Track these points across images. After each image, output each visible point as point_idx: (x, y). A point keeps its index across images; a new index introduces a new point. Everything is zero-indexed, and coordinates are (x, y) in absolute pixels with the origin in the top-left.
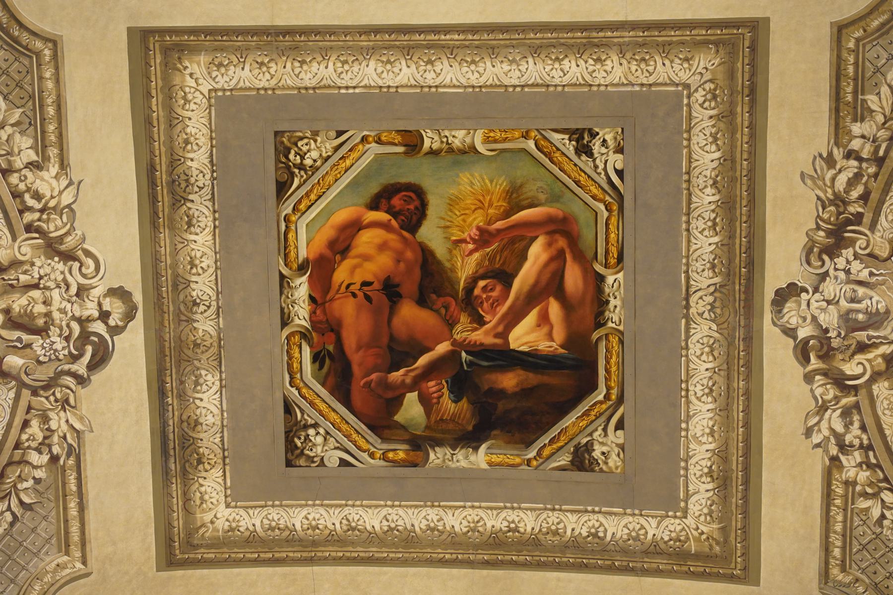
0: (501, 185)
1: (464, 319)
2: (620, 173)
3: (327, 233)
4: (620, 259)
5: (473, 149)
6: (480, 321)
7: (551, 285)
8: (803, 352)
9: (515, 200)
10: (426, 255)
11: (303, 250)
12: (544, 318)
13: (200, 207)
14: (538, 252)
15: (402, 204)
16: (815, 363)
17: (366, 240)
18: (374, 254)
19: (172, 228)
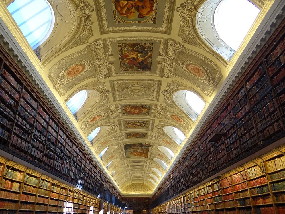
0: (129, 18)
1: (133, 4)
2: (115, 20)
3: (150, 14)
4: (114, 11)
5: (132, 21)
6: (131, 4)
7: (122, 8)
8: (89, 5)
9: (127, 17)
10: (138, 11)
11: (154, 13)
12: (123, 4)
13: (166, 18)
14: (124, 11)
15: (141, 16)
16: (87, 4)
17: (146, 13)
18: (144, 12)
19: (169, 16)
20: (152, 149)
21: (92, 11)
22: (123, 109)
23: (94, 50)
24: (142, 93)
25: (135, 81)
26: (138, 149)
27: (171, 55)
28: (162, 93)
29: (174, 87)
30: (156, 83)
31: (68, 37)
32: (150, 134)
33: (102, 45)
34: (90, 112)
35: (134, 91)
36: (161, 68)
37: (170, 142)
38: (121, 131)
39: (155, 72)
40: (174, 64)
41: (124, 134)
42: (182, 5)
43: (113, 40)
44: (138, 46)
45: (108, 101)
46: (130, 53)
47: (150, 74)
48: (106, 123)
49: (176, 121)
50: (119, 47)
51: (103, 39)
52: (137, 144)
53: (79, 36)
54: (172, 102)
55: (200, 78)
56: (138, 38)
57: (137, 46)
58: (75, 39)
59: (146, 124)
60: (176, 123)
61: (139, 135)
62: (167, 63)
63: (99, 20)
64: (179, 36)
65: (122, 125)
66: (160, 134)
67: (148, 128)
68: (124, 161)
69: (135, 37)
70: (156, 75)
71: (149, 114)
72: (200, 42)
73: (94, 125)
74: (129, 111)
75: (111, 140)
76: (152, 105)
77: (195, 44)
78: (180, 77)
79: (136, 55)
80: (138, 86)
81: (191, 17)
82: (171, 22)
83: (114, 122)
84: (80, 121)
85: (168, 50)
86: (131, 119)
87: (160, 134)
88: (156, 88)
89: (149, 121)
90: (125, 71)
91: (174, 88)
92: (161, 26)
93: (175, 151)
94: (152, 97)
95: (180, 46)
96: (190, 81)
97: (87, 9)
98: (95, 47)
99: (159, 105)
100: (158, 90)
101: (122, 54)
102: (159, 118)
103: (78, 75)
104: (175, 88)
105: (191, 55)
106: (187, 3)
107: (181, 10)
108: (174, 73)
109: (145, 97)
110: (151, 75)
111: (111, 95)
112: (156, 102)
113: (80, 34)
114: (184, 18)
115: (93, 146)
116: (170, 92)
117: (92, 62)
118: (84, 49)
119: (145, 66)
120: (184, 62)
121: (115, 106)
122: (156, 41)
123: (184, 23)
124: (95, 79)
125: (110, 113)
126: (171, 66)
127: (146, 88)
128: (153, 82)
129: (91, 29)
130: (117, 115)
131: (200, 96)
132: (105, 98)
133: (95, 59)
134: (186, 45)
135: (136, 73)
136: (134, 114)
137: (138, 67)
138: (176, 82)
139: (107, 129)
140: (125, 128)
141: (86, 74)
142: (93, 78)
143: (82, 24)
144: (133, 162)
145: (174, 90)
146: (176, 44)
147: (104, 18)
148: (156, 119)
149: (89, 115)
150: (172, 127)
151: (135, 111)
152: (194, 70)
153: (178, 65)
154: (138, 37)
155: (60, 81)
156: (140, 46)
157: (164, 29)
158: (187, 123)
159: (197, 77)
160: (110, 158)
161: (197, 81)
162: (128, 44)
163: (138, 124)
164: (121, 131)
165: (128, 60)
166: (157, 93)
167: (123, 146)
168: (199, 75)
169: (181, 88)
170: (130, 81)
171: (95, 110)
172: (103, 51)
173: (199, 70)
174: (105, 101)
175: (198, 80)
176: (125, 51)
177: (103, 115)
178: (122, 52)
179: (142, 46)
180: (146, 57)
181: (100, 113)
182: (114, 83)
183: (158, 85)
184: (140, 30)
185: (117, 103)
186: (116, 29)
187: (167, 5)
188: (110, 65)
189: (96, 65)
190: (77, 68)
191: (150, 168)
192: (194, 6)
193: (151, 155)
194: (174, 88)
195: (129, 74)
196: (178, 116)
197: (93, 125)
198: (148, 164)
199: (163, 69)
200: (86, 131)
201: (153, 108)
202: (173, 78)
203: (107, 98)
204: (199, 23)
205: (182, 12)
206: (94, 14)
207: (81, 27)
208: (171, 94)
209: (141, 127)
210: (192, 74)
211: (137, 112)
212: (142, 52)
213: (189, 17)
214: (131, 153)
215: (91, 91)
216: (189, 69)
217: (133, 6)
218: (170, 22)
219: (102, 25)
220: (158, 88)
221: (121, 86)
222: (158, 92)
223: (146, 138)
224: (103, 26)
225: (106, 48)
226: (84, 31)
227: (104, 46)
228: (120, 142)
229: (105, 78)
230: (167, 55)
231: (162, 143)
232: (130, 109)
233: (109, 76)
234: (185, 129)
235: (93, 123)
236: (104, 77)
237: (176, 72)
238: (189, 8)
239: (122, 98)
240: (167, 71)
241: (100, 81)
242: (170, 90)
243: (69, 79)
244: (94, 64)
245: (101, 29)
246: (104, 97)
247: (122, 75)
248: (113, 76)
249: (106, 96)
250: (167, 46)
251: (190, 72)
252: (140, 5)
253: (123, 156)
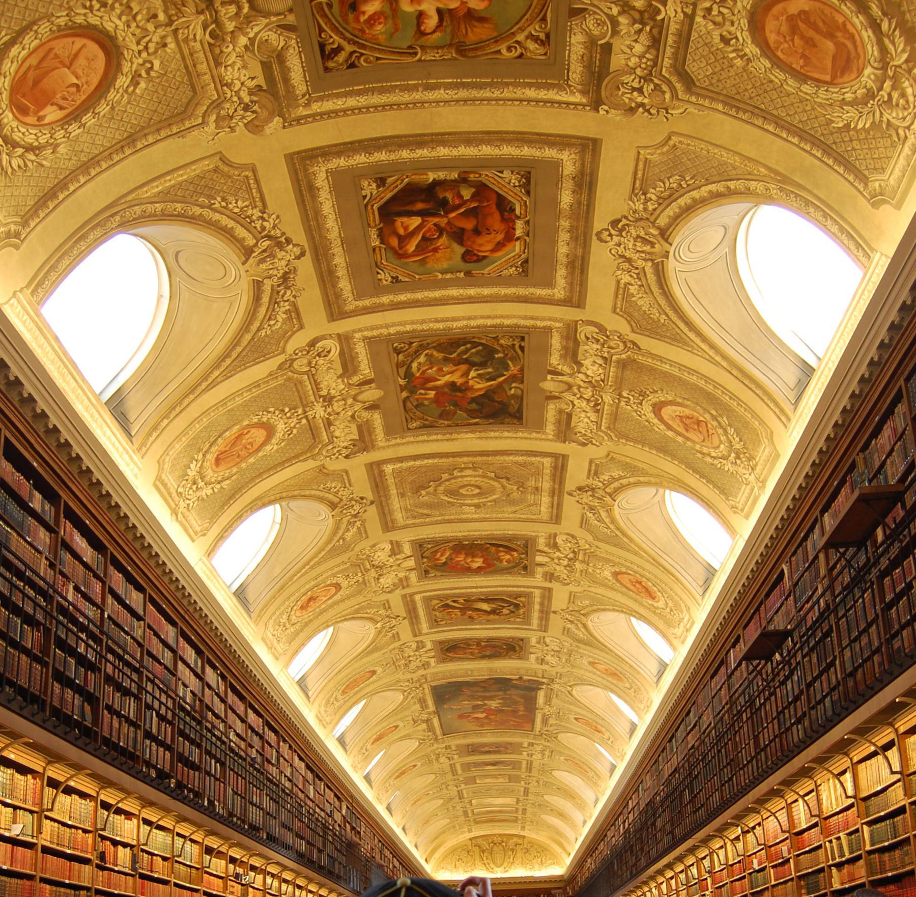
0: (429, 266)
1: (443, 225)
2: (378, 273)
3: (506, 249)
4: (374, 250)
5: (442, 274)
6: (435, 225)
8: (288, 241)
9: (423, 262)
10: (461, 242)
11: (518, 246)
12: (406, 228)
14: (411, 247)
16: (283, 239)
17: (490, 247)
18: (484, 244)
19: (576, 256)
20: (548, 700)
21: (298, 258)
22: (423, 557)
23: (306, 373)
24: (491, 498)
25: (465, 459)
26: (491, 698)
27: (593, 372)
28: (570, 494)
29: (616, 474)
30: (547, 462)
31: (218, 346)
32: (539, 643)
33: (335, 354)
34: (295, 578)
35: (463, 491)
36: (561, 412)
37: (620, 676)
38: (415, 636)
39: (539, 425)
40: (607, 399)
41: (429, 646)
42: (615, 223)
43: (375, 333)
44: (469, 346)
45: (363, 533)
46: (440, 370)
47: (520, 434)
48: (357, 611)
49: (634, 595)
50: (398, 354)
51: (339, 335)
52: (485, 681)
53: (253, 338)
54: (612, 527)
55: (705, 450)
56: (465, 323)
57: (463, 348)
58: (239, 349)
59: (517, 606)
60: (636, 600)
61: (493, 647)
62: (581, 397)
63: (323, 281)
64: (614, 312)
65: (421, 612)
66: (579, 641)
67: (527, 620)
68: (436, 746)
69: (454, 319)
70: (543, 437)
71: (527, 570)
72: (692, 335)
73: (311, 621)
74: (445, 564)
75: (379, 670)
76: (537, 536)
77: (675, 339)
78: (636, 441)
79: (462, 376)
80: (475, 476)
81: (652, 260)
82: (584, 270)
83: (386, 605)
84: (260, 616)
85: (580, 357)
86: (456, 588)
87: (579, 641)
88: (547, 478)
89: (529, 596)
90: (425, 426)
91: (615, 479)
92: (549, 283)
93: (642, 707)
94: (534, 508)
95: (624, 343)
96: (674, 456)
97: (280, 254)
98: (310, 363)
99: (565, 537)
100: (557, 486)
101: (408, 375)
102: (568, 584)
103: (252, 460)
104: (621, 478)
105: (666, 375)
106: (631, 219)
107: (616, 239)
108: (609, 428)
109: (508, 512)
110: (526, 435)
111: (373, 511)
112: (552, 528)
113: (259, 330)
114: (629, 260)
115: (308, 697)
116: (602, 491)
117: (300, 411)
118: (270, 375)
119: (498, 410)
120: (643, 394)
121: (388, 547)
122: (535, 327)
123: (631, 276)
124: (311, 464)
125: (373, 573)
126: (596, 405)
127: (508, 479)
128: (533, 459)
129: (295, 313)
130: (401, 580)
131: (714, 511)
132: (349, 523)
133: (312, 398)
134: (645, 342)
135: (466, 432)
136: (468, 571)
137: (472, 414)
138: (623, 459)
139: (361, 632)
140: (435, 623)
141: (277, 451)
142: (304, 460)
143: (265, 299)
144: (474, 749)
145: (616, 484)
146: (607, 337)
147: (341, 272)
148: (554, 585)
149: (292, 589)
150: (623, 615)
151: (469, 560)
152: (682, 422)
153: (623, 404)
154: (464, 318)
155: (191, 492)
156: (475, 345)
157: (559, 291)
158: (676, 605)
159: (698, 447)
160: (377, 740)
161: (698, 458)
162: (429, 341)
163: (485, 606)
164: (415, 636)
165: (432, 394)
166: (553, 497)
167: (427, 691)
168: (703, 441)
169: (642, 479)
170: (444, 460)
171: (312, 568)
172: (340, 371)
173: (698, 423)
174: (349, 536)
175: (699, 455)
176: (420, 364)
177: (344, 584)
178: (410, 367)
179: (482, 344)
180: (501, 379)
181: (334, 576)
182: (382, 473)
183: (555, 468)
184: (471, 297)
185: (395, 536)
186: (385, 299)
187: (565, 224)
188: (366, 415)
189: (315, 417)
190: (247, 436)
191: (544, 770)
192: (659, 228)
193: (545, 721)
194: (615, 479)
195: (440, 437)
196: (643, 576)
197: (306, 625)
198: (537, 757)
199: (570, 416)
200: (280, 647)
201: (541, 547)
202: (608, 446)
203: (358, 524)
204: (684, 275)
205: (619, 245)
206: (306, 266)
207: (262, 310)
208: (608, 499)
209: (497, 617)
210: (680, 434)
211: (478, 562)
212: (483, 365)
213: (645, 260)
214: (461, 717)
215: (293, 504)
216: (665, 417)
217: (441, 231)
218: (578, 271)
219: (335, 294)
220: (554, 480)
221: (411, 479)
222: (557, 492)
223: (520, 658)
224: (338, 295)
225: (348, 365)
226: (270, 319)
227: (342, 354)
228: (415, 676)
229: (347, 457)
230: (579, 372)
231: (587, 674)
232: (450, 555)
233: (364, 450)
234: (669, 624)
235: (307, 615)
236: (345, 452)
237: (617, 425)
238: (642, 234)
239: (414, 517)
240: (583, 421)
241: (331, 468)
242: (601, 485)
243: (220, 478)
244: (306, 418)
245: (330, 305)
246: (345, 520)
247: (413, 442)
248: (379, 449)
249: (355, 516)
250: (577, 343)
251: (669, 427)
252: (469, 225)
253: (431, 729)
